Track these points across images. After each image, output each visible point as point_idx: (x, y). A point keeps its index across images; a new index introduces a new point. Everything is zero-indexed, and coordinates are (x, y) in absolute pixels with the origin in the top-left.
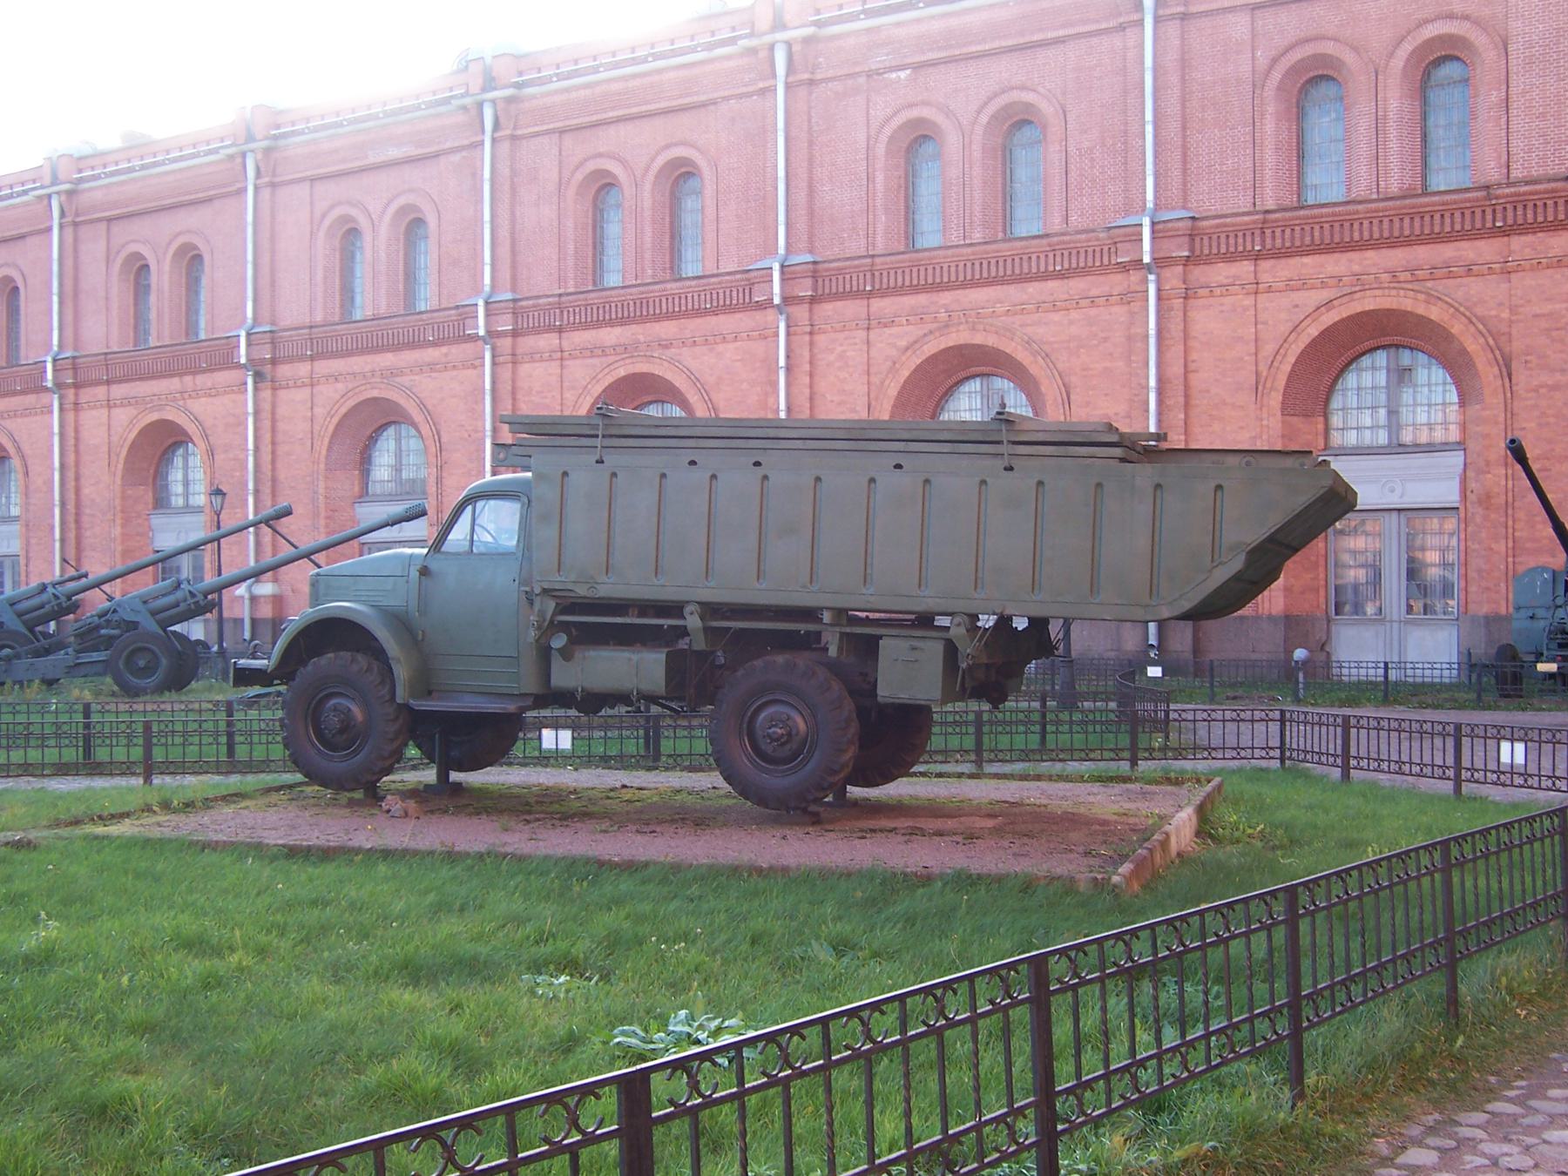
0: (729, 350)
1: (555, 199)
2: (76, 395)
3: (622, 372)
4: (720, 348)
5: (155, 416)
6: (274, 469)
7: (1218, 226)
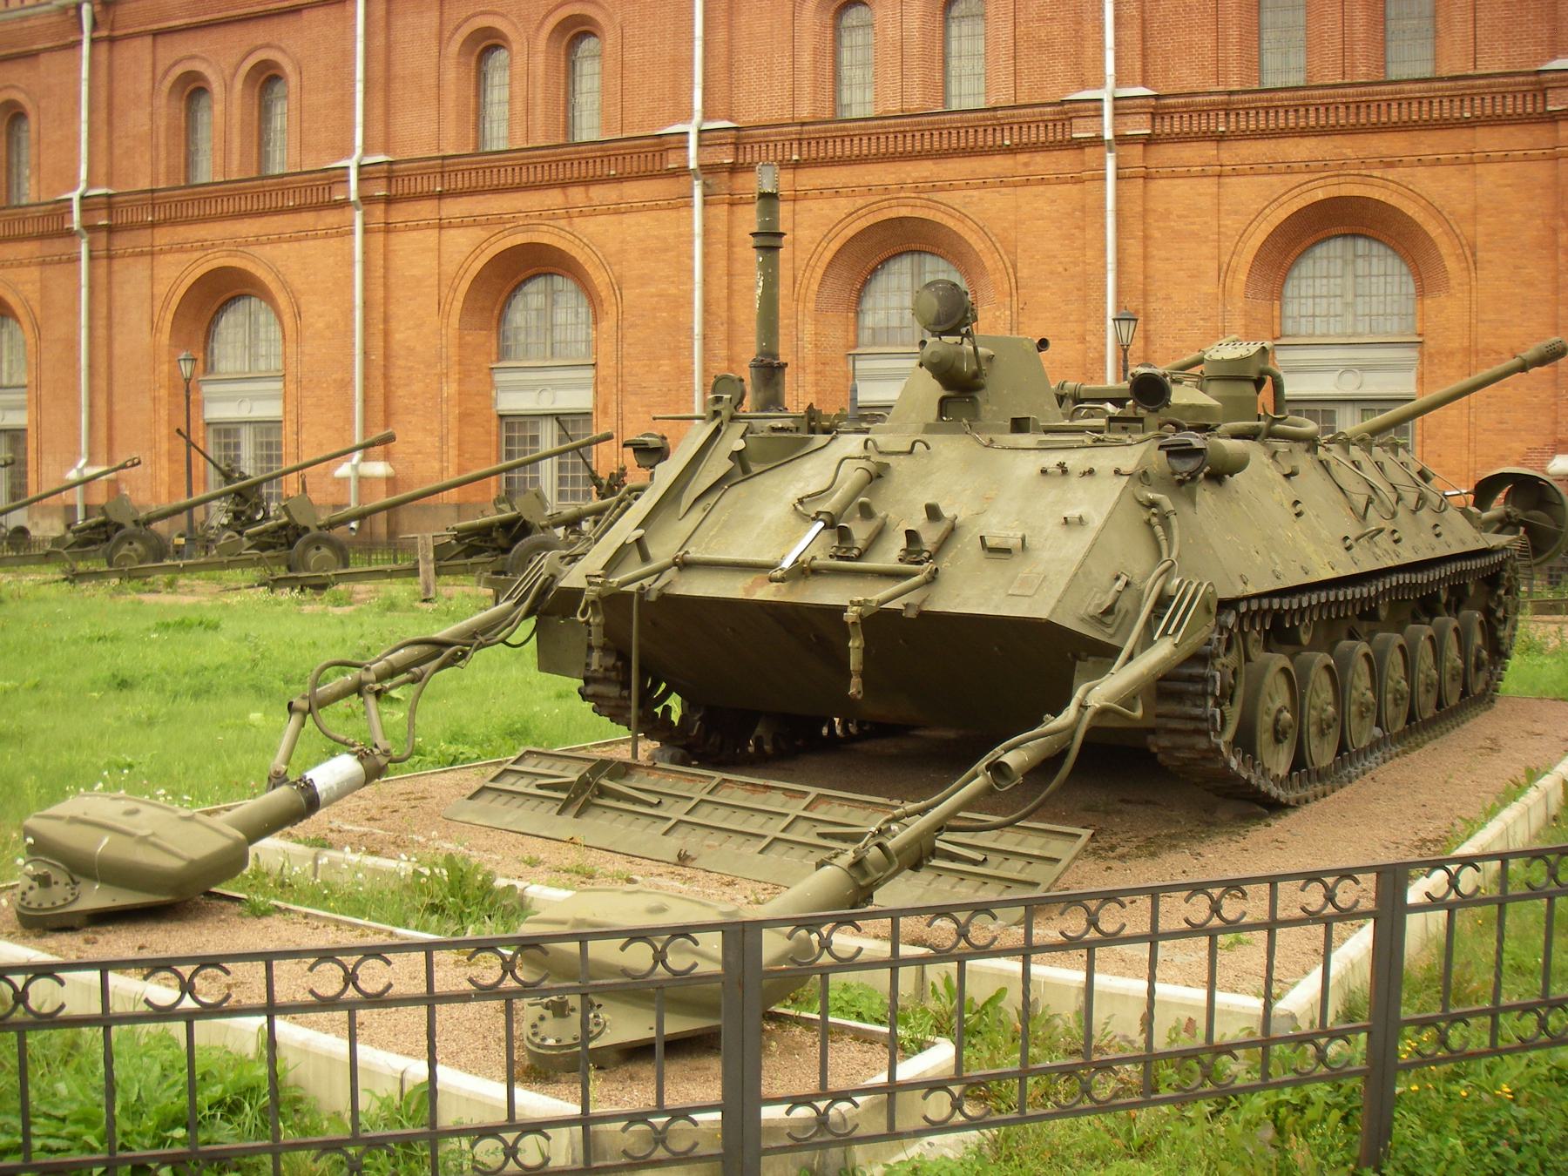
0: (1491, 175)
2: (109, 242)
3: (1320, 195)
4: (1480, 169)
5: (520, 239)
6: (730, 308)
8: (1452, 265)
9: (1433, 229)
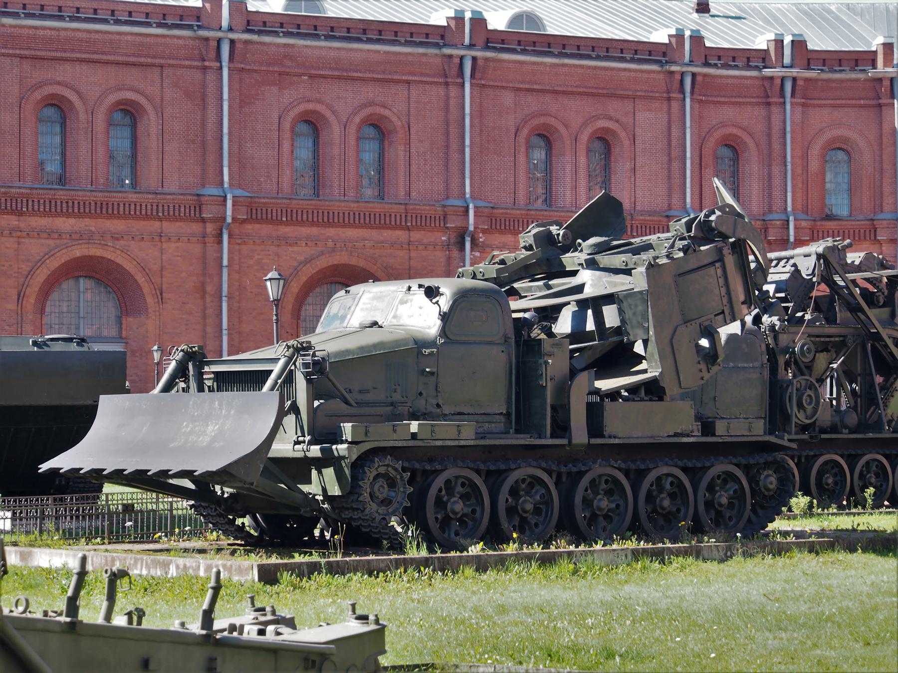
0: (171, 248)
1: (17, 109)
7: (502, 213)
8: (150, 300)
9: (140, 278)
